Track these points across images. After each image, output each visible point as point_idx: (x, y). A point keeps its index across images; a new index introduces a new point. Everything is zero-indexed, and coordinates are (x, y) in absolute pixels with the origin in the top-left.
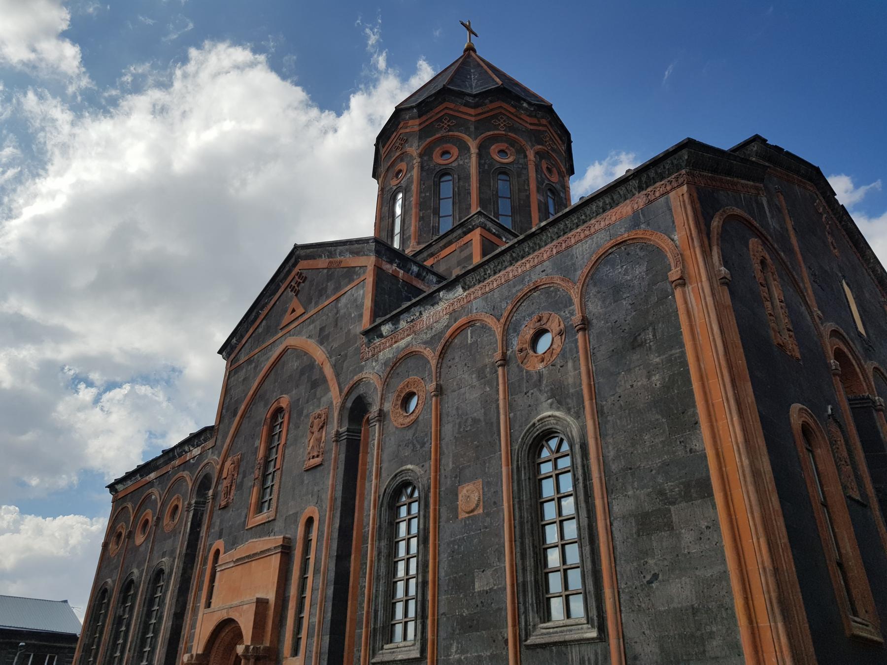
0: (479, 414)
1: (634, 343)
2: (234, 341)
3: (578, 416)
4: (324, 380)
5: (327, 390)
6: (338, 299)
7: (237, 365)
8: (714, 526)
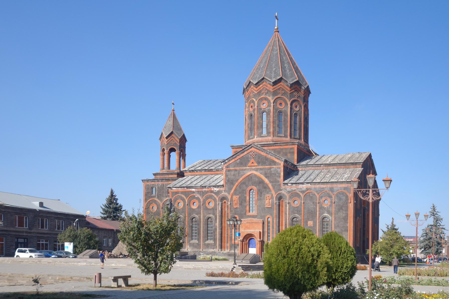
0: (313, 210)
1: (341, 208)
2: (227, 161)
3: (331, 215)
4: (269, 188)
5: (270, 191)
6: (271, 168)
7: (228, 169)
8: (347, 235)
